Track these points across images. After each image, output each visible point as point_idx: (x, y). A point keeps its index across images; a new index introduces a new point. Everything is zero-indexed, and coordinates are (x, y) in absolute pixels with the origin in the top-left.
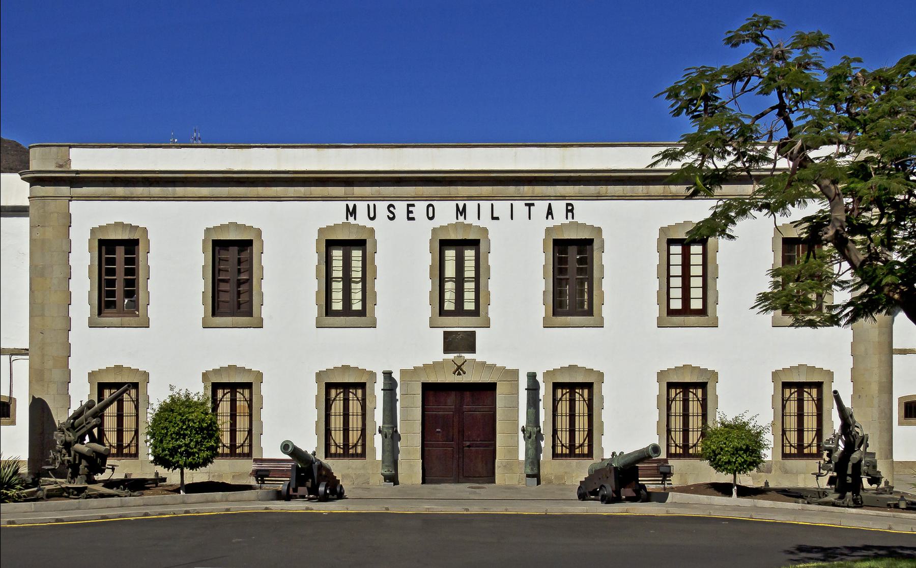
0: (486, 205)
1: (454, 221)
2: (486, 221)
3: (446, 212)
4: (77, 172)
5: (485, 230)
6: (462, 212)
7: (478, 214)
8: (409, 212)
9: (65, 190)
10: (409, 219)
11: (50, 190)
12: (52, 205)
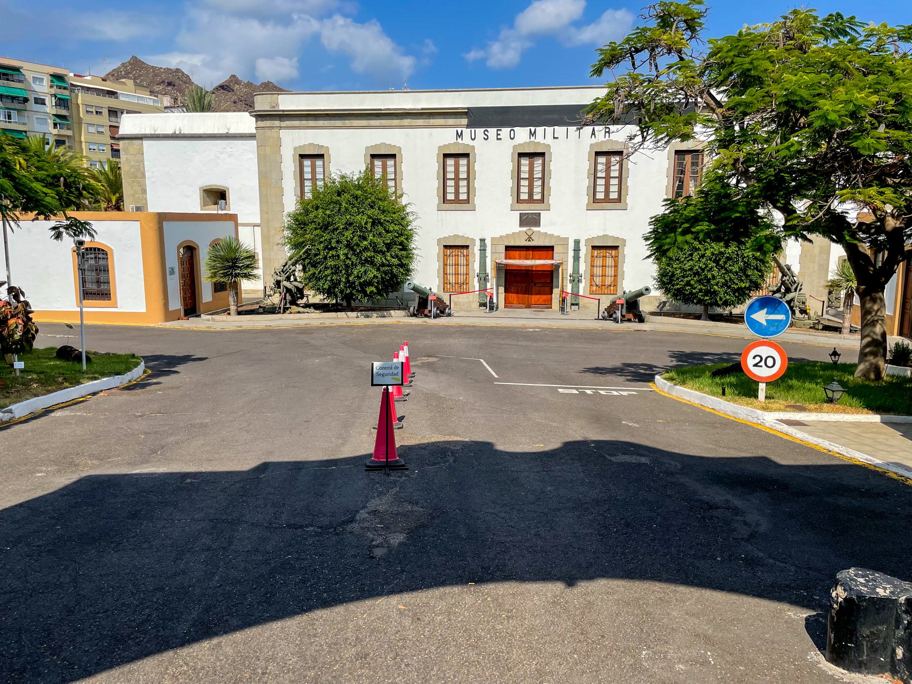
0: (549, 130)
1: (528, 140)
2: (549, 140)
3: (522, 134)
4: (283, 111)
5: (549, 146)
6: (533, 134)
7: (544, 136)
8: (498, 135)
9: (277, 123)
10: (498, 139)
11: (268, 123)
12: (268, 133)
